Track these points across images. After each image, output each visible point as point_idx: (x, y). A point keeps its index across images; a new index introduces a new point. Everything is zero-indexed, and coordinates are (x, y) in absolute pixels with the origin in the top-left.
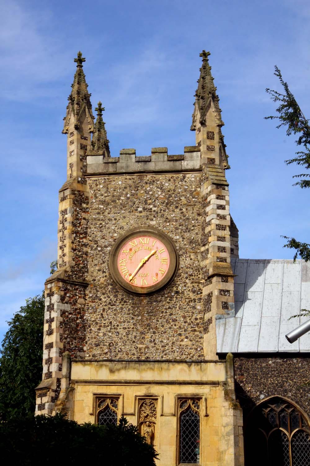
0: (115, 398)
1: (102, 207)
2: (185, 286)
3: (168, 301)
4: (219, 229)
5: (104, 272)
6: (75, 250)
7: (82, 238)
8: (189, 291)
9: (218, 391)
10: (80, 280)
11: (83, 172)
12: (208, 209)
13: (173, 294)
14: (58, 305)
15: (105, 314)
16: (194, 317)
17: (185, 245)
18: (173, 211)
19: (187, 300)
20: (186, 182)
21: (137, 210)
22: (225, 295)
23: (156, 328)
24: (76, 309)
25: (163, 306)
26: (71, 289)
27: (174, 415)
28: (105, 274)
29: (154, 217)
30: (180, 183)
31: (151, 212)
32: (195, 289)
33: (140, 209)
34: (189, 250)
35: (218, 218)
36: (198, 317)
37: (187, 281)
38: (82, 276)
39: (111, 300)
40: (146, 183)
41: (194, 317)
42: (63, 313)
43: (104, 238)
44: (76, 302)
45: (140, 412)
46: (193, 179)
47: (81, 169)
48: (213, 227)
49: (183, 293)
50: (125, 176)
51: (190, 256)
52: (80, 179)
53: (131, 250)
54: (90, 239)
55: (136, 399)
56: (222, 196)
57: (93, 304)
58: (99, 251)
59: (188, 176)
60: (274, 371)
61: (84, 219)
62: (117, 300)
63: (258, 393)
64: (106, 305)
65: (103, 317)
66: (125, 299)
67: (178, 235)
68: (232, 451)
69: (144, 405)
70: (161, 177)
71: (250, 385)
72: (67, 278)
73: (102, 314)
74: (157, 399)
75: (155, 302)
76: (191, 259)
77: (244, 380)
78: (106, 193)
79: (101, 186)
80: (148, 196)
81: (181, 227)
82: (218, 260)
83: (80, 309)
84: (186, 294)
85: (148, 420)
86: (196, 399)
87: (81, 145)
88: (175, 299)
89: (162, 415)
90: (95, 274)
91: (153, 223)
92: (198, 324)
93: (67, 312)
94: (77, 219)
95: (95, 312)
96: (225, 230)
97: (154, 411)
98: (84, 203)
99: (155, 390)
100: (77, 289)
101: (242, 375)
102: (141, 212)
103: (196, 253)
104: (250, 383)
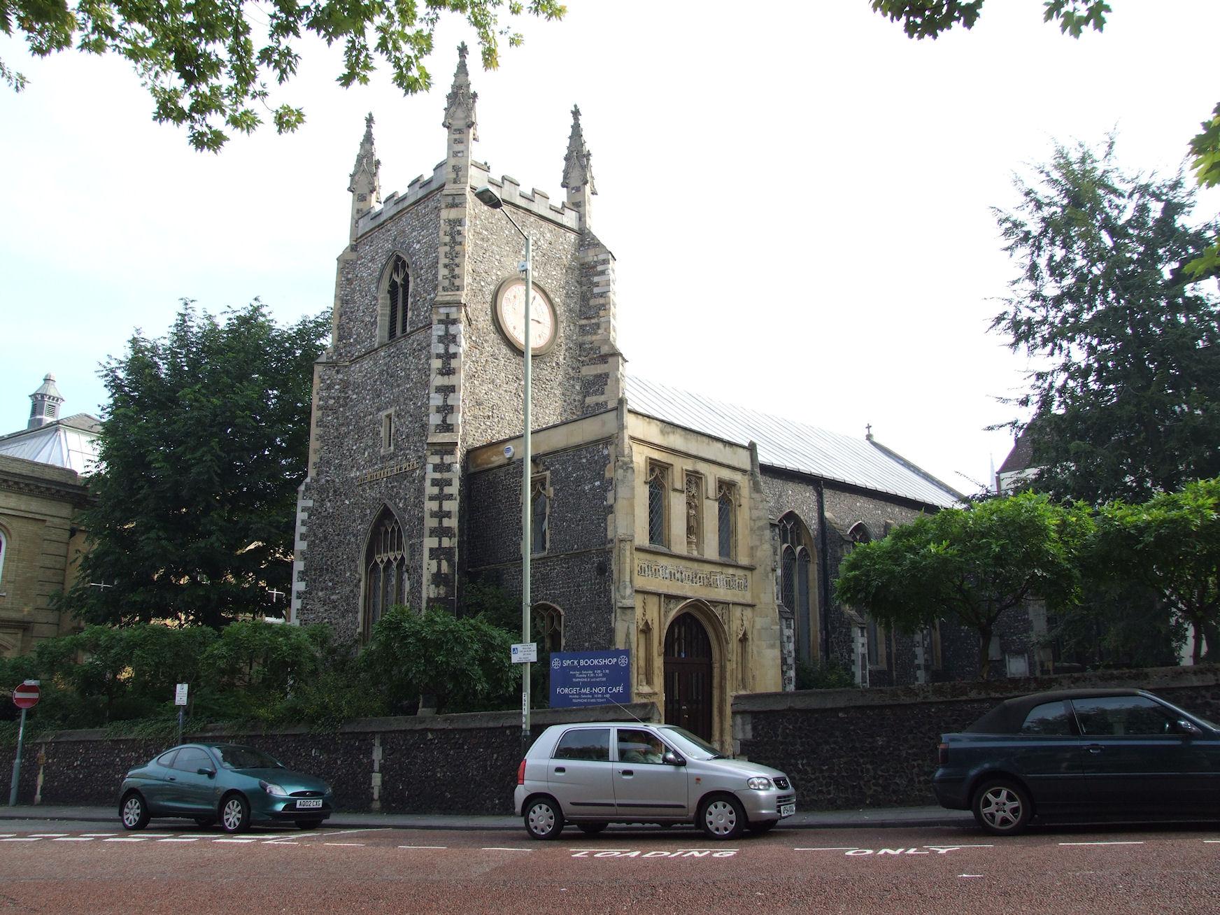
36: (577, 399)
99: (702, 467)
103: (575, 324)
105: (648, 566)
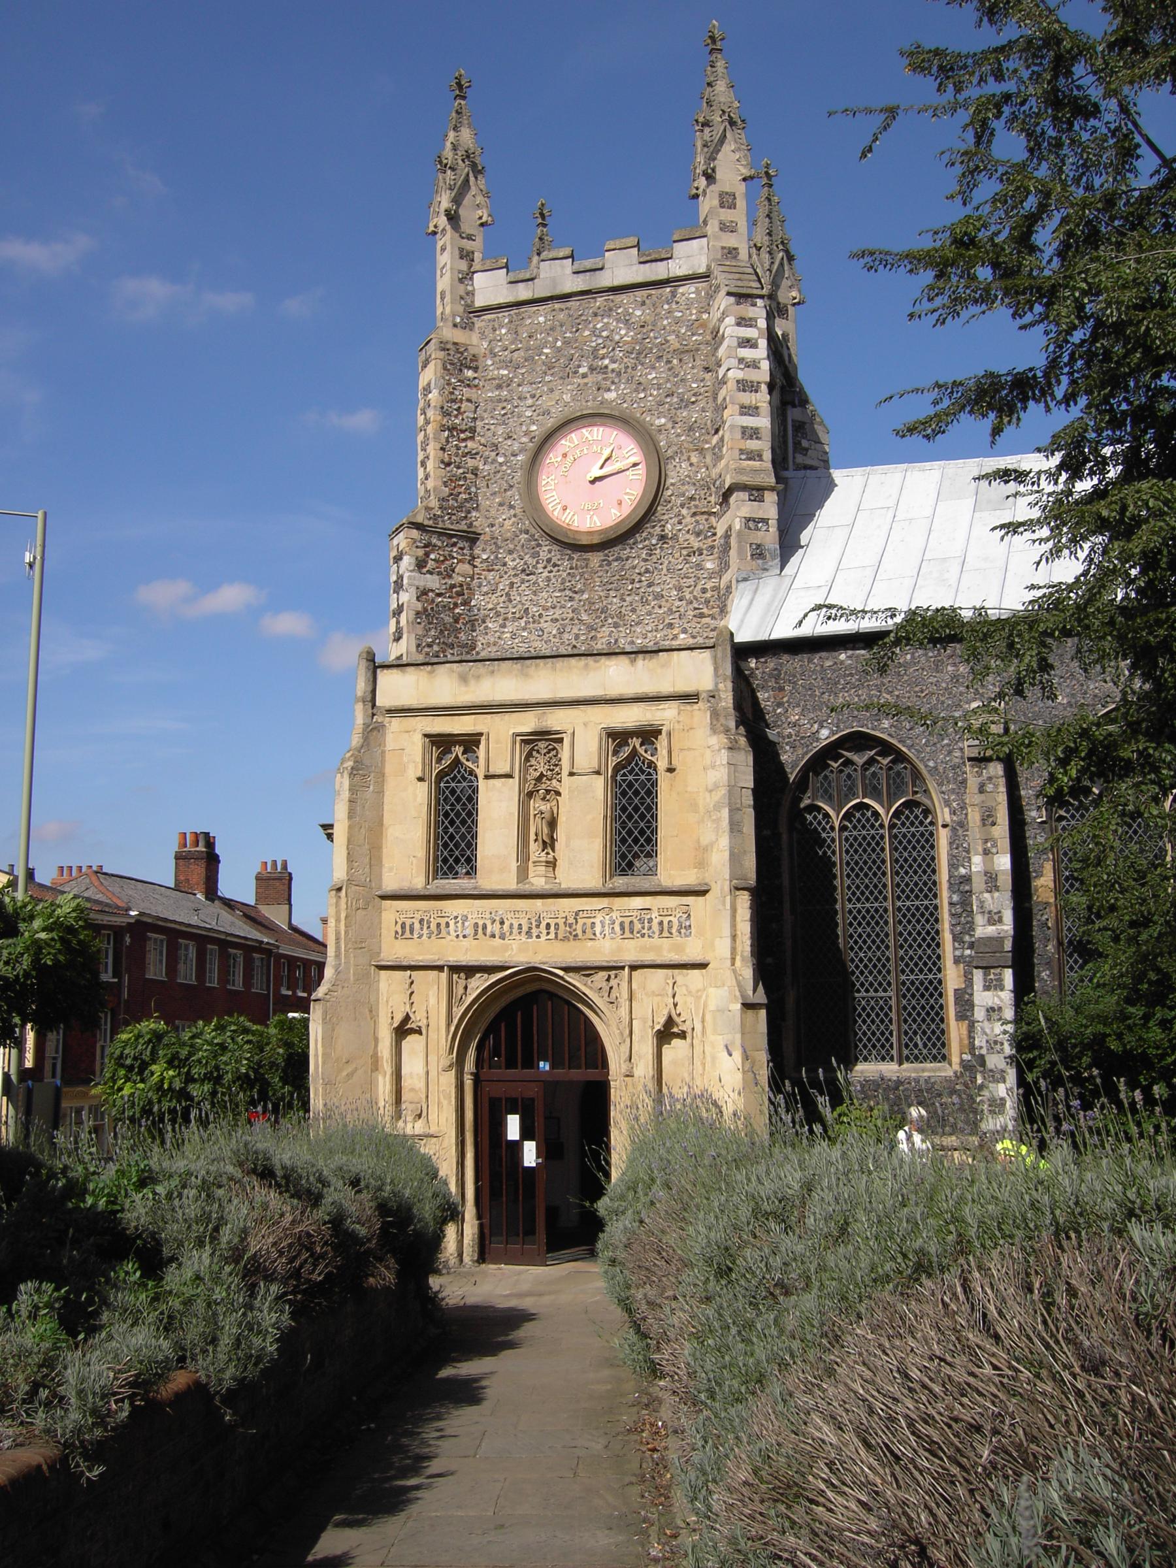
0: (471, 742)
1: (506, 372)
2: (680, 523)
3: (644, 556)
4: (744, 391)
5: (511, 507)
6: (448, 464)
7: (464, 440)
8: (688, 532)
9: (697, 713)
10: (463, 526)
11: (467, 306)
12: (721, 352)
13: (654, 542)
14: (409, 578)
15: (513, 593)
16: (699, 587)
17: (678, 435)
18: (654, 368)
19: (685, 552)
20: (677, 303)
21: (576, 372)
22: (758, 529)
23: (621, 615)
24: (453, 586)
25: (634, 567)
26: (439, 544)
27: (598, 773)
28: (512, 512)
29: (613, 383)
30: (666, 307)
31: (605, 373)
32: (701, 527)
33: (582, 370)
34: (686, 445)
35: (742, 366)
36: (708, 586)
37: (684, 511)
38: (466, 517)
39: (525, 563)
40: (596, 315)
41: (699, 587)
42: (423, 593)
43: (510, 437)
44: (453, 571)
45: (525, 769)
46: (693, 296)
47: (462, 298)
48: (732, 385)
49: (675, 537)
50: (551, 305)
51: (689, 459)
52: (458, 320)
53: (565, 455)
54: (483, 441)
55: (514, 743)
56: (751, 319)
57: (490, 576)
58: (501, 464)
59: (681, 290)
60: (851, 675)
61: (469, 400)
62: (538, 562)
63: (816, 726)
64: (515, 575)
65: (510, 601)
66: (554, 560)
67: (665, 417)
68: (724, 842)
69: (534, 753)
70: (624, 298)
71: (797, 710)
72: (430, 523)
73: (508, 594)
74: (561, 740)
75: (616, 560)
76: (691, 465)
77: (785, 699)
78: (512, 343)
79: (503, 331)
80: (600, 341)
81: (668, 400)
82: (743, 457)
83: (461, 585)
84: (681, 540)
85: (544, 786)
86: (649, 735)
87: (461, 250)
88: (658, 551)
89: (571, 774)
90: (493, 512)
91: (611, 396)
92: (707, 602)
93: (432, 591)
94: (454, 401)
95: (494, 592)
96: (756, 391)
97: (556, 765)
98: (469, 368)
99: (556, 720)
100: (454, 545)
101: (782, 689)
102: (584, 376)
103: (701, 451)
104: (798, 705)
105: (421, 921)
